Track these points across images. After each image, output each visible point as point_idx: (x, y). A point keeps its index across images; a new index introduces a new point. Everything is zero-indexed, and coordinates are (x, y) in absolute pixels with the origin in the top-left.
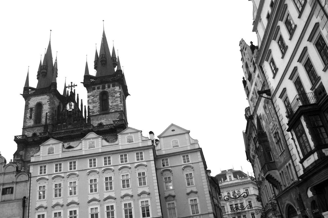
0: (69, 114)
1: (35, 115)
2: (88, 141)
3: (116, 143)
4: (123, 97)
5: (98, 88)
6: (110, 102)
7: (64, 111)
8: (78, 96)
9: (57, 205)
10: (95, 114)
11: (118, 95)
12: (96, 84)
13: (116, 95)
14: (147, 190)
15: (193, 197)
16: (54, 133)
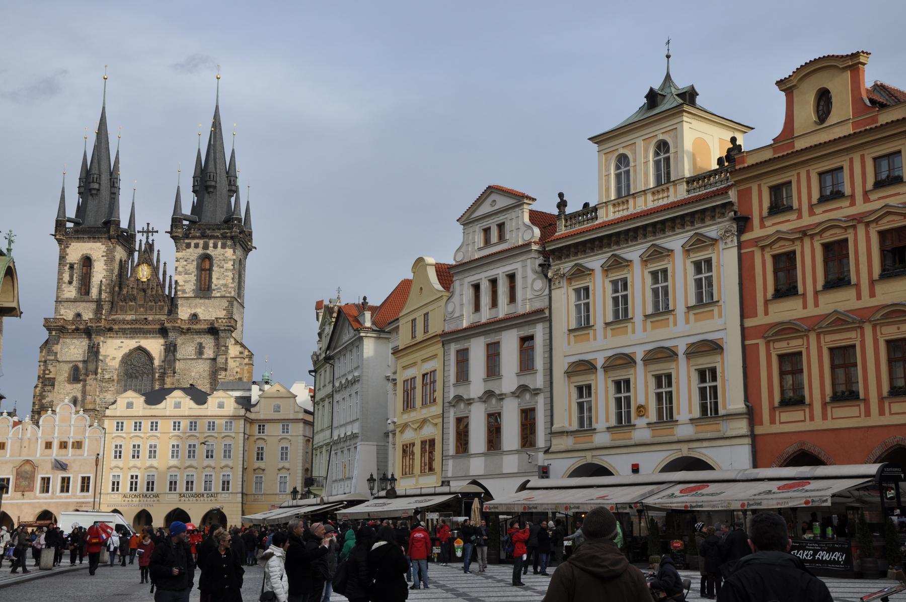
0: (140, 286)
1: (79, 280)
2: (173, 400)
3: (205, 406)
4: (240, 260)
5: (196, 246)
6: (215, 276)
7: (132, 279)
8: (158, 254)
9: (135, 467)
10: (187, 295)
11: (229, 265)
12: (194, 238)
13: (225, 265)
14: (230, 463)
15: (283, 473)
16: (114, 320)
